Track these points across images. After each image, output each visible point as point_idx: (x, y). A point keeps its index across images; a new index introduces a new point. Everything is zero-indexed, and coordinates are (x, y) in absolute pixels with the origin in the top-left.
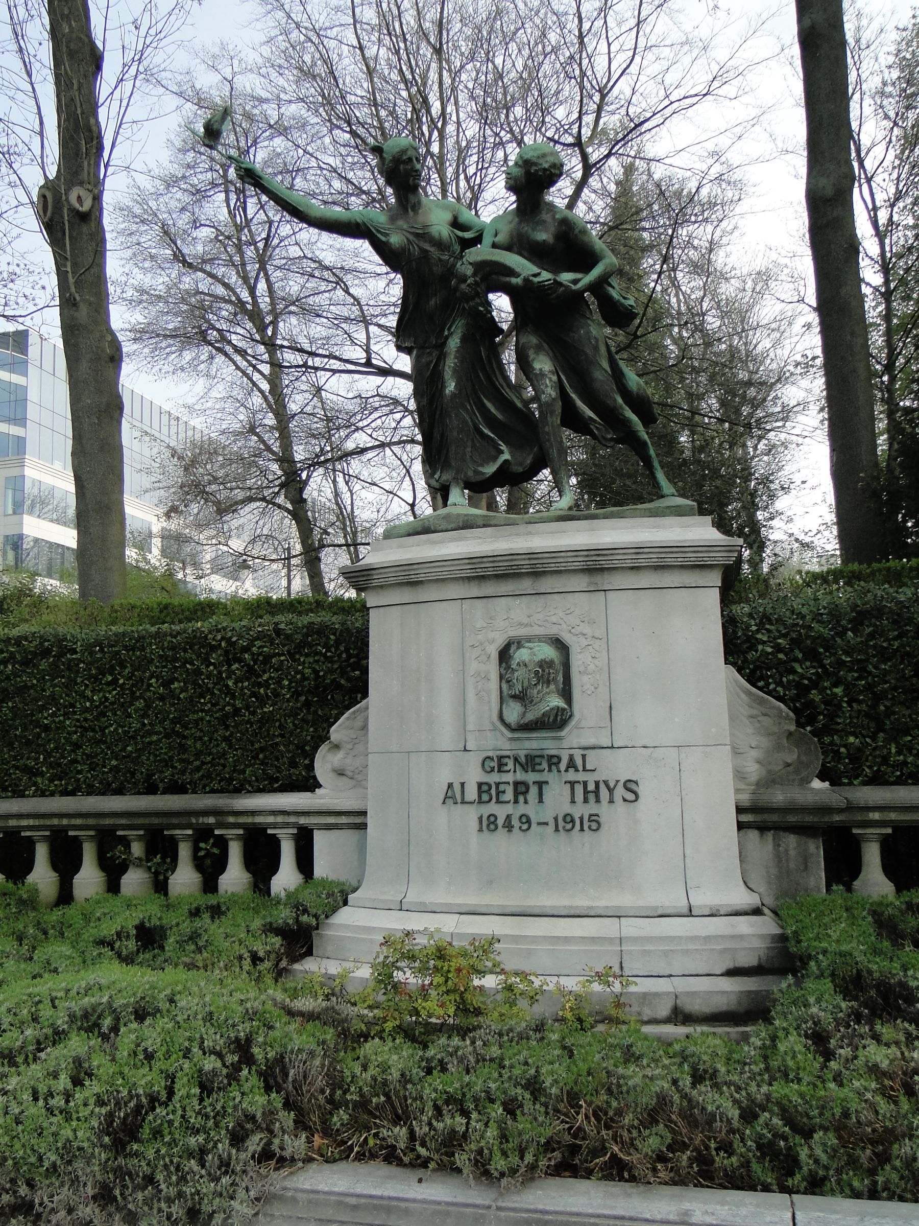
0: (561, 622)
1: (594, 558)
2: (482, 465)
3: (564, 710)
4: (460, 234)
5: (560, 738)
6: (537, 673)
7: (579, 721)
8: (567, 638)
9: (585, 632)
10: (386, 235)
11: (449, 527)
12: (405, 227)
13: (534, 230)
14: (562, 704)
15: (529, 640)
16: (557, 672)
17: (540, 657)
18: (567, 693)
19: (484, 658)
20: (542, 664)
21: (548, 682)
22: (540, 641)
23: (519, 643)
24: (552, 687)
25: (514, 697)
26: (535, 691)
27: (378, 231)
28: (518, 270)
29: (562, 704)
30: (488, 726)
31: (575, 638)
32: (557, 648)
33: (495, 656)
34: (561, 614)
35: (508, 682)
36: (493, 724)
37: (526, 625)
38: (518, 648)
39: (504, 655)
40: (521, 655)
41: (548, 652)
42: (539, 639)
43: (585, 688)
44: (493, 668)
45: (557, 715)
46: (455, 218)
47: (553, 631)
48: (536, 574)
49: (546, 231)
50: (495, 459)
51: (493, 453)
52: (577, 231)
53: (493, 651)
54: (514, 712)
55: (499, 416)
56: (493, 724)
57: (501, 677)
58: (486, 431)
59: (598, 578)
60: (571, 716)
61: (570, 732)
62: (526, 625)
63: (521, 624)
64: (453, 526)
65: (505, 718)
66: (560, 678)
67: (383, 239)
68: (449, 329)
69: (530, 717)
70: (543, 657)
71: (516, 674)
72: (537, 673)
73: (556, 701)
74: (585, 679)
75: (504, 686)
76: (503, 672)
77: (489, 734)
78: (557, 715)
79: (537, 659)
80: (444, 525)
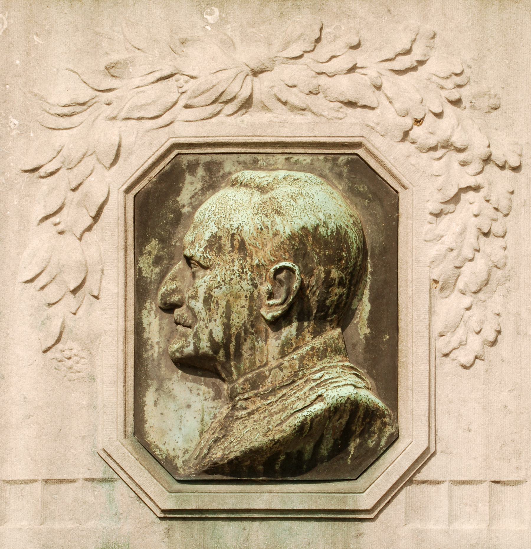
7: (425, 458)
8: (392, 157)
14: (369, 396)
15: (257, 152)
19: (77, 217)
23: (211, 168)
30: (82, 463)
36: (105, 457)
38: (211, 186)
44: (108, 253)
47: (345, 127)
53: (113, 187)
54: (186, 416)
56: (105, 457)
57: (142, 291)
60: (394, 439)
65: (152, 437)
70: (309, 221)
71: (204, 281)
75: (154, 323)
76: (150, 272)
79: (286, 227)
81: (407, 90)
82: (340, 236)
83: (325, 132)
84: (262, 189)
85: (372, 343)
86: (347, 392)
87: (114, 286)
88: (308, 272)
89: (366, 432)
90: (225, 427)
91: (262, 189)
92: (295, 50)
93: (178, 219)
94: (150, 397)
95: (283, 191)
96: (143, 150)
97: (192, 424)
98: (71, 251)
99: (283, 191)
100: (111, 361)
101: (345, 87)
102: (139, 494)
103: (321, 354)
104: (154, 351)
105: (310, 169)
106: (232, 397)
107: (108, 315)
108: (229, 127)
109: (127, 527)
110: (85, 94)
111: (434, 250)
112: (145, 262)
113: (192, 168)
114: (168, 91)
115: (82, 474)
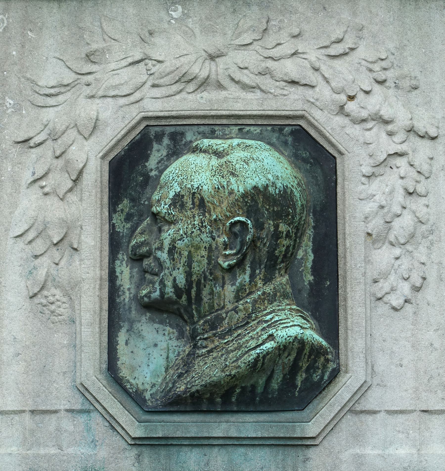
0: (313, 78)
3: (317, 351)
5: (302, 444)
6: (236, 231)
7: (363, 390)
8: (331, 127)
9: (386, 113)
14: (312, 336)
15: (215, 125)
16: (297, 234)
17: (251, 179)
18: (323, 301)
19: (60, 181)
20: (258, 201)
21: (271, 267)
22: (242, 133)
24: (282, 280)
25: (157, 308)
26: (229, 290)
29: (312, 336)
30: (62, 396)
31: (356, 131)
32: (296, 159)
33: (96, 176)
34: (313, 56)
35: (137, 258)
36: (83, 391)
37: (204, 84)
38: (175, 153)
39: (129, 171)
40: (194, 171)
41: (267, 166)
42: (241, 125)
43: (385, 286)
45: (294, 368)
47: (290, 102)
53: (92, 156)
54: (152, 354)
56: (83, 391)
57: (115, 243)
60: (335, 374)
61: (332, 426)
62: (204, 84)
63: (185, 79)
65: (124, 373)
66: (306, 254)
69: (210, 370)
71: (169, 234)
72: (236, 231)
73: (292, 326)
74: (384, 256)
75: (125, 273)
76: (123, 228)
77: (67, 424)
78: (294, 368)
79: (238, 187)
81: (343, 72)
82: (286, 195)
83: (272, 106)
84: (218, 154)
85: (316, 288)
86: (294, 331)
87: (92, 240)
88: (259, 226)
89: (311, 369)
90: (187, 363)
91: (218, 154)
92: (246, 38)
93: (149, 182)
94: (122, 337)
95: (237, 156)
96: (116, 124)
97: (158, 361)
98: (55, 210)
99: (237, 156)
100: (91, 304)
101: (291, 68)
102: (113, 424)
103: (271, 298)
104: (126, 298)
105: (259, 137)
106: (193, 336)
107: (88, 265)
108: (190, 103)
109: (103, 453)
110: (69, 77)
111: (369, 207)
112: (118, 219)
113: (159, 138)
114: (139, 74)
115: (63, 405)
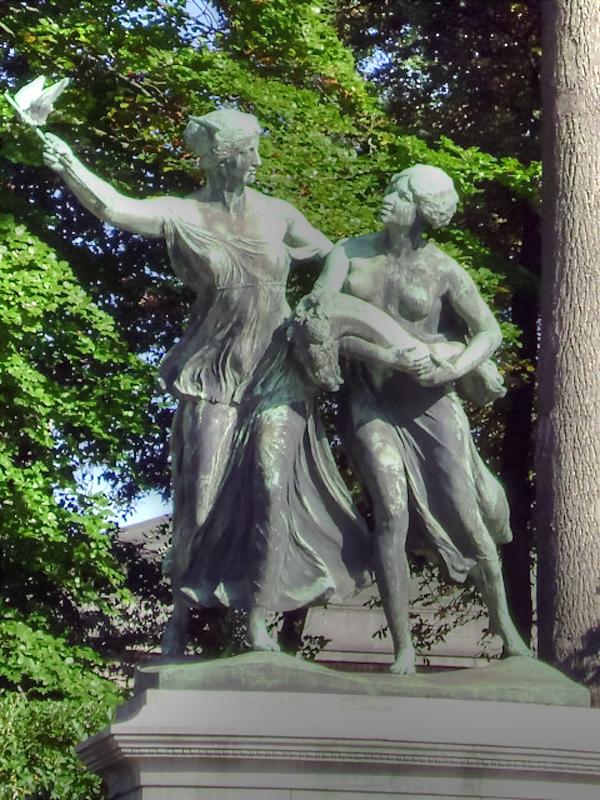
1: (478, 755)
2: (290, 588)
4: (291, 250)
10: (201, 245)
11: (270, 684)
12: (229, 238)
13: (409, 281)
27: (188, 235)
28: (387, 337)
46: (289, 228)
48: (398, 769)
49: (426, 285)
50: (311, 581)
51: (308, 573)
52: (463, 291)
55: (316, 519)
58: (303, 541)
59: (476, 782)
64: (275, 682)
67: (197, 250)
68: (263, 385)
80: (262, 680)
